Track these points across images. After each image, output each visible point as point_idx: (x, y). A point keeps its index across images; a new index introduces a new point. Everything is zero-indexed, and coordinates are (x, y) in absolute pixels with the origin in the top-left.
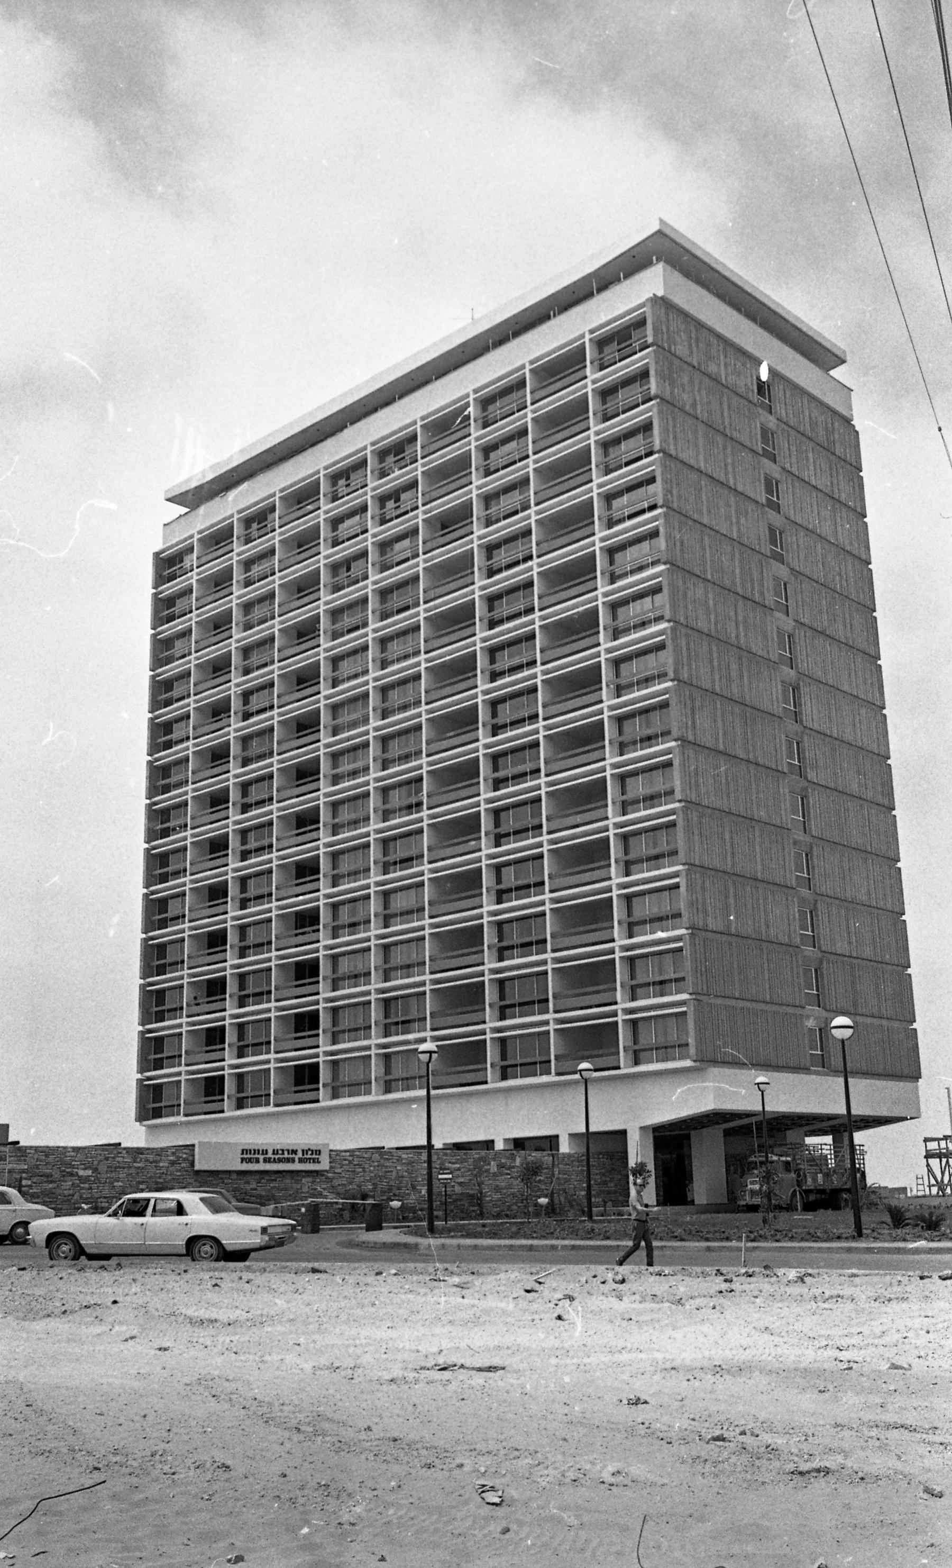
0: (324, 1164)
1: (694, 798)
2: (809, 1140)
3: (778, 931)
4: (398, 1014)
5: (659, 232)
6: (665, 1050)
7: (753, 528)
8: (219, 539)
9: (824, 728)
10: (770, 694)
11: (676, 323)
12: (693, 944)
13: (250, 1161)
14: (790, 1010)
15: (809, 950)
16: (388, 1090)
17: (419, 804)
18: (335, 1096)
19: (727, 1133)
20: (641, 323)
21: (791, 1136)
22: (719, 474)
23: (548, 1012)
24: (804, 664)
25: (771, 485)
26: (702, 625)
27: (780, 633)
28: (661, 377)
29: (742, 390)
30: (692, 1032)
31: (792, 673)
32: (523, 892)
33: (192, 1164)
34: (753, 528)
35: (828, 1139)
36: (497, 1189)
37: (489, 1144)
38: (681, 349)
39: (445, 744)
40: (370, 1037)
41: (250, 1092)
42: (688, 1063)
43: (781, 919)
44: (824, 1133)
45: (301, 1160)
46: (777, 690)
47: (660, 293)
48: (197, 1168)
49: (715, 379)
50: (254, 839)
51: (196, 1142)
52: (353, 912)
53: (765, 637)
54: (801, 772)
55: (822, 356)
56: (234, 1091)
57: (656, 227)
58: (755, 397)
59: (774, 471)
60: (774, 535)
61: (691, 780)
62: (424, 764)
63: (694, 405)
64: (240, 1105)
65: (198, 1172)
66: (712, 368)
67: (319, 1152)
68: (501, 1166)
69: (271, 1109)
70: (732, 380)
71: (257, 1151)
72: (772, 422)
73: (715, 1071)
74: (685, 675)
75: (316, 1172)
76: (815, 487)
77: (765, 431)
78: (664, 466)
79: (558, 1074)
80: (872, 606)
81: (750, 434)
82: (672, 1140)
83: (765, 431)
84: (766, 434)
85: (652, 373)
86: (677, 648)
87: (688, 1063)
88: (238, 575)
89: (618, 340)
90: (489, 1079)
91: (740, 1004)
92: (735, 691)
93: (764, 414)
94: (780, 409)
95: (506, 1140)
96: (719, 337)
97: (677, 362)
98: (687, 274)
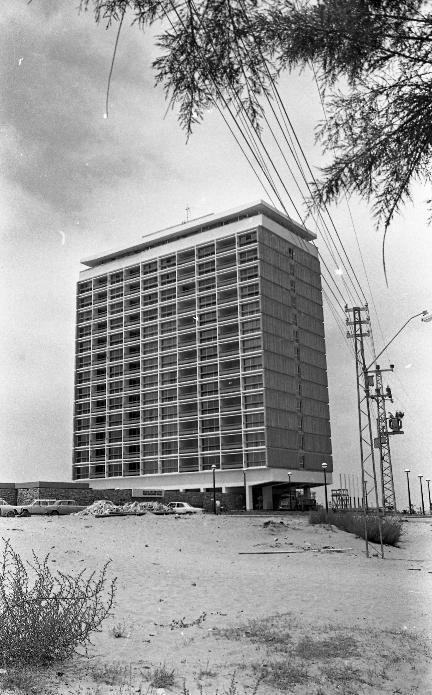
0: (163, 496)
1: (268, 387)
2: (297, 490)
3: (291, 427)
4: (168, 448)
5: (261, 204)
6: (257, 464)
7: (286, 299)
8: (102, 281)
9: (306, 361)
10: (290, 352)
11: (266, 235)
12: (267, 431)
13: (145, 494)
14: (294, 451)
15: (300, 432)
16: (163, 472)
17: (175, 380)
18: (144, 474)
19: (273, 488)
20: (255, 232)
21: (292, 489)
22: (277, 282)
23: (219, 449)
24: (300, 342)
25: (293, 284)
26: (271, 332)
27: (294, 332)
28: (261, 253)
29: (284, 253)
30: (266, 457)
31: (297, 344)
32: (211, 411)
33: (131, 495)
34: (286, 299)
35: (302, 490)
36: (206, 504)
37: (199, 490)
38: (266, 242)
39: (185, 362)
40: (157, 455)
41: (115, 471)
42: (265, 467)
43: (293, 423)
44: (302, 488)
45: (158, 494)
46: (293, 350)
47: (261, 224)
48: (132, 496)
49: (276, 251)
50: (116, 388)
51: (132, 488)
52: (151, 414)
53: (289, 333)
54: (299, 376)
55: (308, 236)
56: (108, 471)
57: (260, 202)
58: (288, 255)
59: (293, 278)
60: (294, 299)
61: (267, 380)
62: (177, 368)
63: (270, 261)
64: (110, 475)
65: (132, 498)
66: (276, 247)
67: (161, 492)
68: (207, 497)
69: (121, 477)
70: (282, 250)
71: (147, 492)
72: (293, 262)
73: (272, 470)
74: (266, 348)
75: (160, 498)
76: (306, 283)
77: (291, 265)
78: (261, 281)
79: (223, 469)
80: (321, 319)
81: (285, 267)
82: (257, 490)
83: (291, 265)
84: (292, 267)
85: (258, 251)
86: (264, 339)
87: (265, 467)
88: (109, 295)
89: (247, 238)
90: (199, 469)
91: (280, 449)
92: (281, 352)
93: (291, 260)
94: (295, 258)
95: (204, 489)
96: (279, 237)
97: (265, 247)
98: (269, 217)
